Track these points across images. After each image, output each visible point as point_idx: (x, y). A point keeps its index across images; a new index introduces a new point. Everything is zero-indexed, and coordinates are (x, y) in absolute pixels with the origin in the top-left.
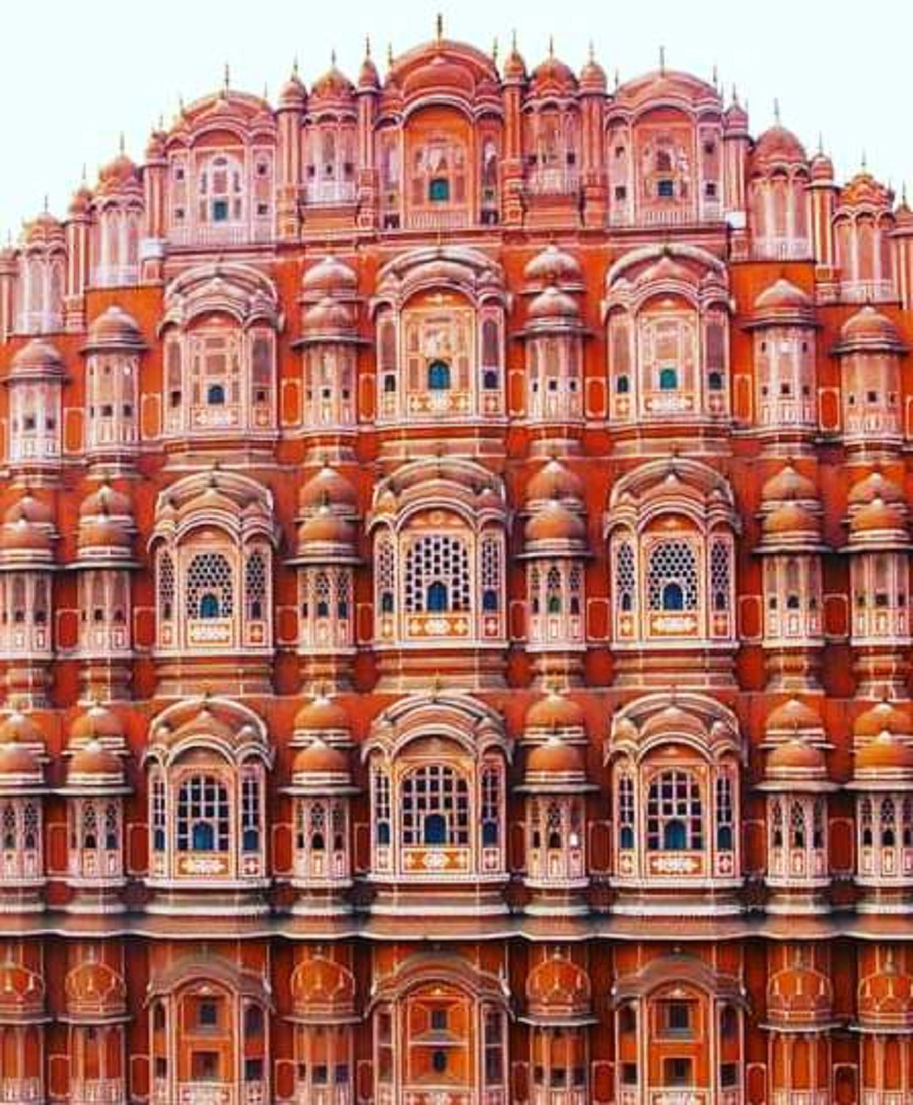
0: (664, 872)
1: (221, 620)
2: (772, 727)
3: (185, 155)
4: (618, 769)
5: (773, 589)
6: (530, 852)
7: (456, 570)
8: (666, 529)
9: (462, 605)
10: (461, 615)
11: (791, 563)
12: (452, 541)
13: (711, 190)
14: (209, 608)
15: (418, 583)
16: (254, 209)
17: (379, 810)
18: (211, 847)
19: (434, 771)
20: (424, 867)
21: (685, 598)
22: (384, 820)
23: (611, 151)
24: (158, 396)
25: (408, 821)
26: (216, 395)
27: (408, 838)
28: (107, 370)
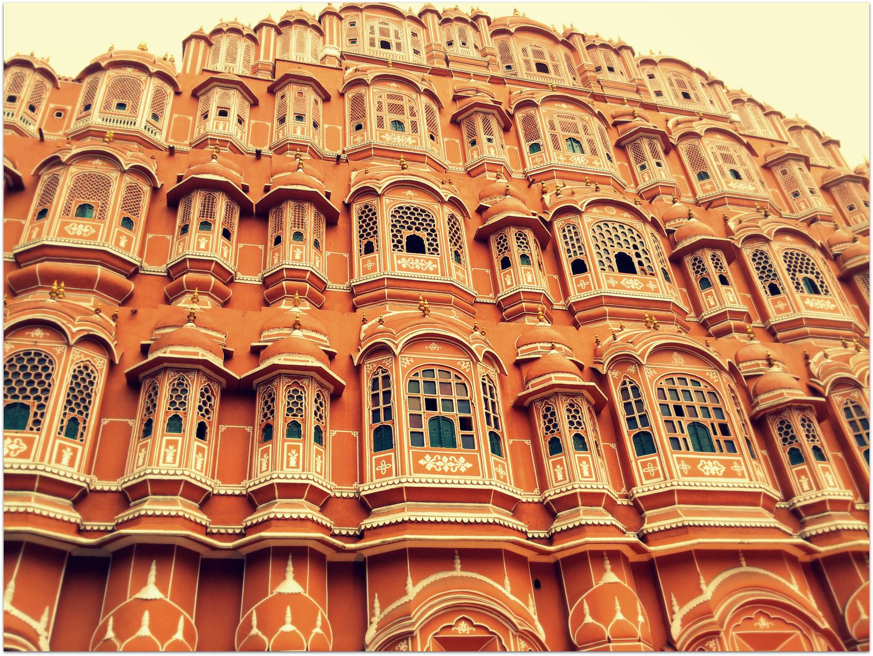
1: (427, 255)
3: (358, 15)
6: (791, 471)
7: (635, 247)
8: (785, 241)
9: (647, 271)
10: (649, 277)
12: (626, 227)
13: (711, 102)
16: (411, 52)
17: (631, 421)
18: (453, 445)
20: (701, 475)
21: (820, 288)
22: (641, 428)
26: (398, 125)
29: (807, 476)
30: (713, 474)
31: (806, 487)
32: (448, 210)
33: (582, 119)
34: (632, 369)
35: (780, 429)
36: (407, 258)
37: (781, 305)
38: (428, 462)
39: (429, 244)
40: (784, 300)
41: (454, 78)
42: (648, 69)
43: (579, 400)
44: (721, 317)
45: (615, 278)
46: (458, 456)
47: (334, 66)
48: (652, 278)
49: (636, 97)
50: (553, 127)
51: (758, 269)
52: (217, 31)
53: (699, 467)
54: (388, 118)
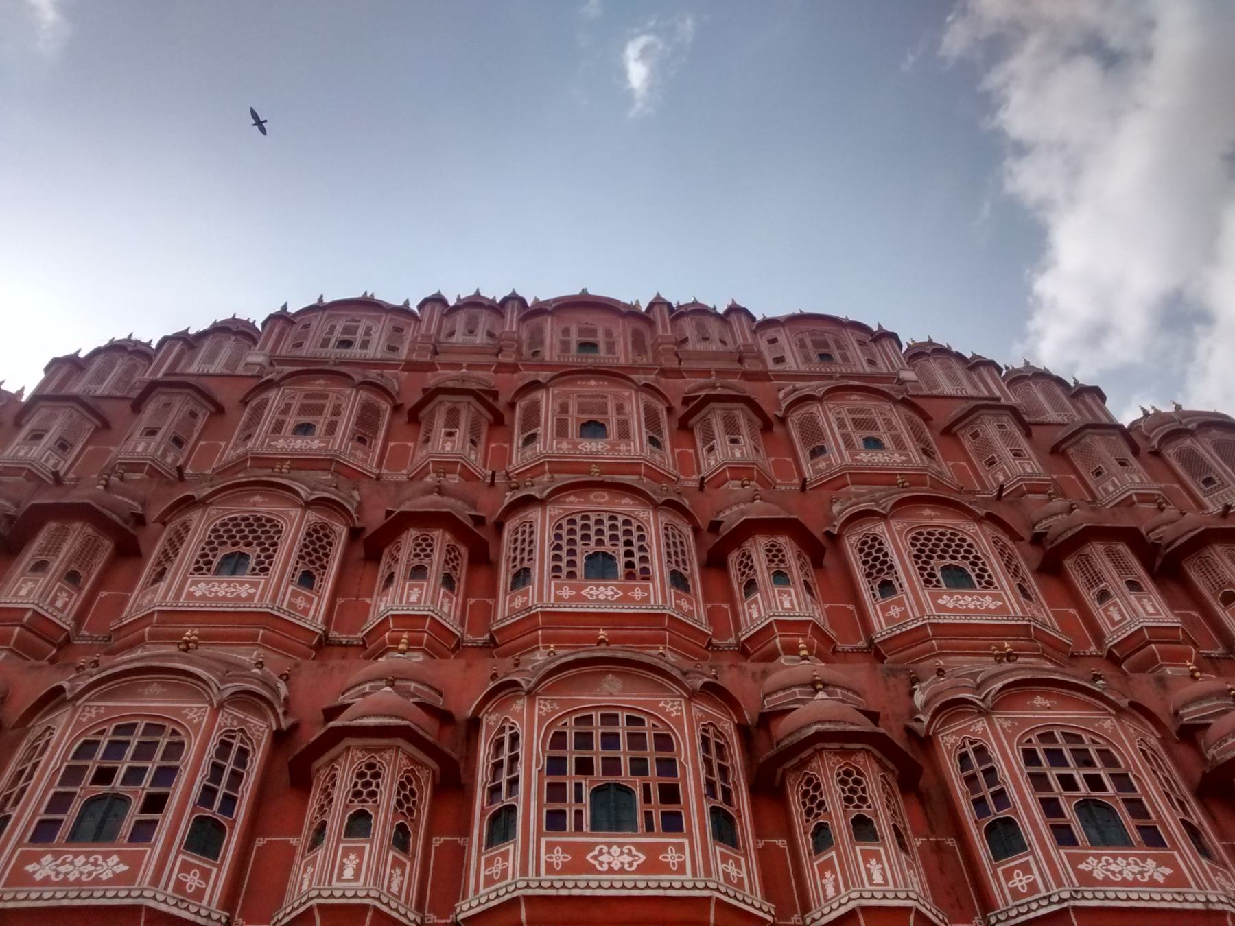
0: (1107, 882)
1: (248, 578)
2: (1186, 704)
4: (948, 741)
5: (1095, 579)
6: (811, 865)
8: (921, 516)
11: (1111, 553)
12: (621, 518)
13: (872, 362)
14: (234, 564)
15: (572, 552)
17: (495, 791)
19: (610, 719)
20: (592, 869)
21: (975, 580)
22: (505, 800)
23: (763, 344)
24: (223, 444)
25: (556, 792)
26: (304, 429)
27: (555, 821)
28: (167, 405)
29: (834, 872)
30: (616, 866)
31: (830, 892)
32: (313, 516)
33: (617, 396)
34: (520, 705)
35: (806, 793)
36: (207, 583)
37: (895, 611)
38: (44, 868)
39: (257, 564)
40: (900, 603)
41: (440, 372)
42: (771, 333)
43: (386, 756)
44: (767, 631)
45: (572, 587)
46: (106, 855)
47: (250, 374)
48: (645, 583)
49: (736, 366)
50: (564, 408)
51: (865, 563)
52: (97, 352)
53: (588, 858)
54: (292, 421)
